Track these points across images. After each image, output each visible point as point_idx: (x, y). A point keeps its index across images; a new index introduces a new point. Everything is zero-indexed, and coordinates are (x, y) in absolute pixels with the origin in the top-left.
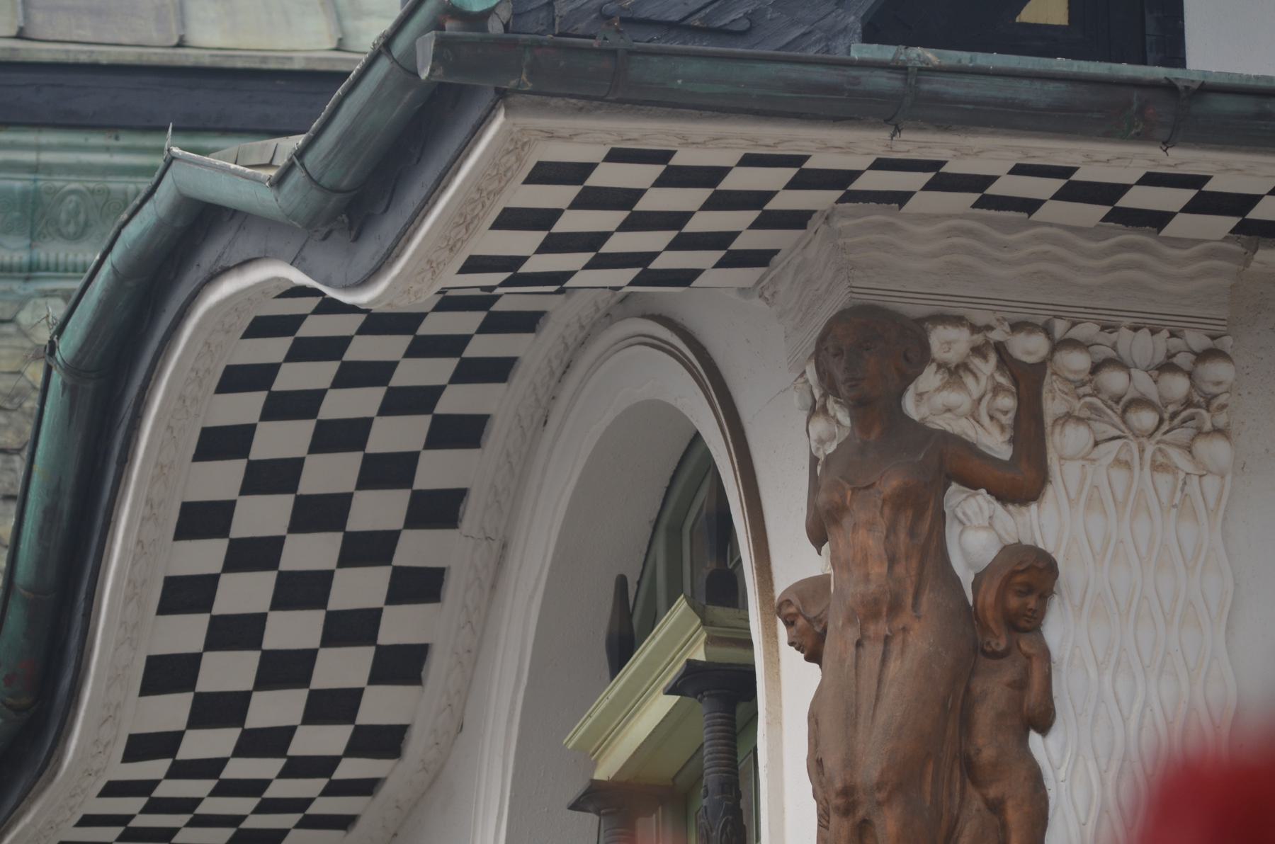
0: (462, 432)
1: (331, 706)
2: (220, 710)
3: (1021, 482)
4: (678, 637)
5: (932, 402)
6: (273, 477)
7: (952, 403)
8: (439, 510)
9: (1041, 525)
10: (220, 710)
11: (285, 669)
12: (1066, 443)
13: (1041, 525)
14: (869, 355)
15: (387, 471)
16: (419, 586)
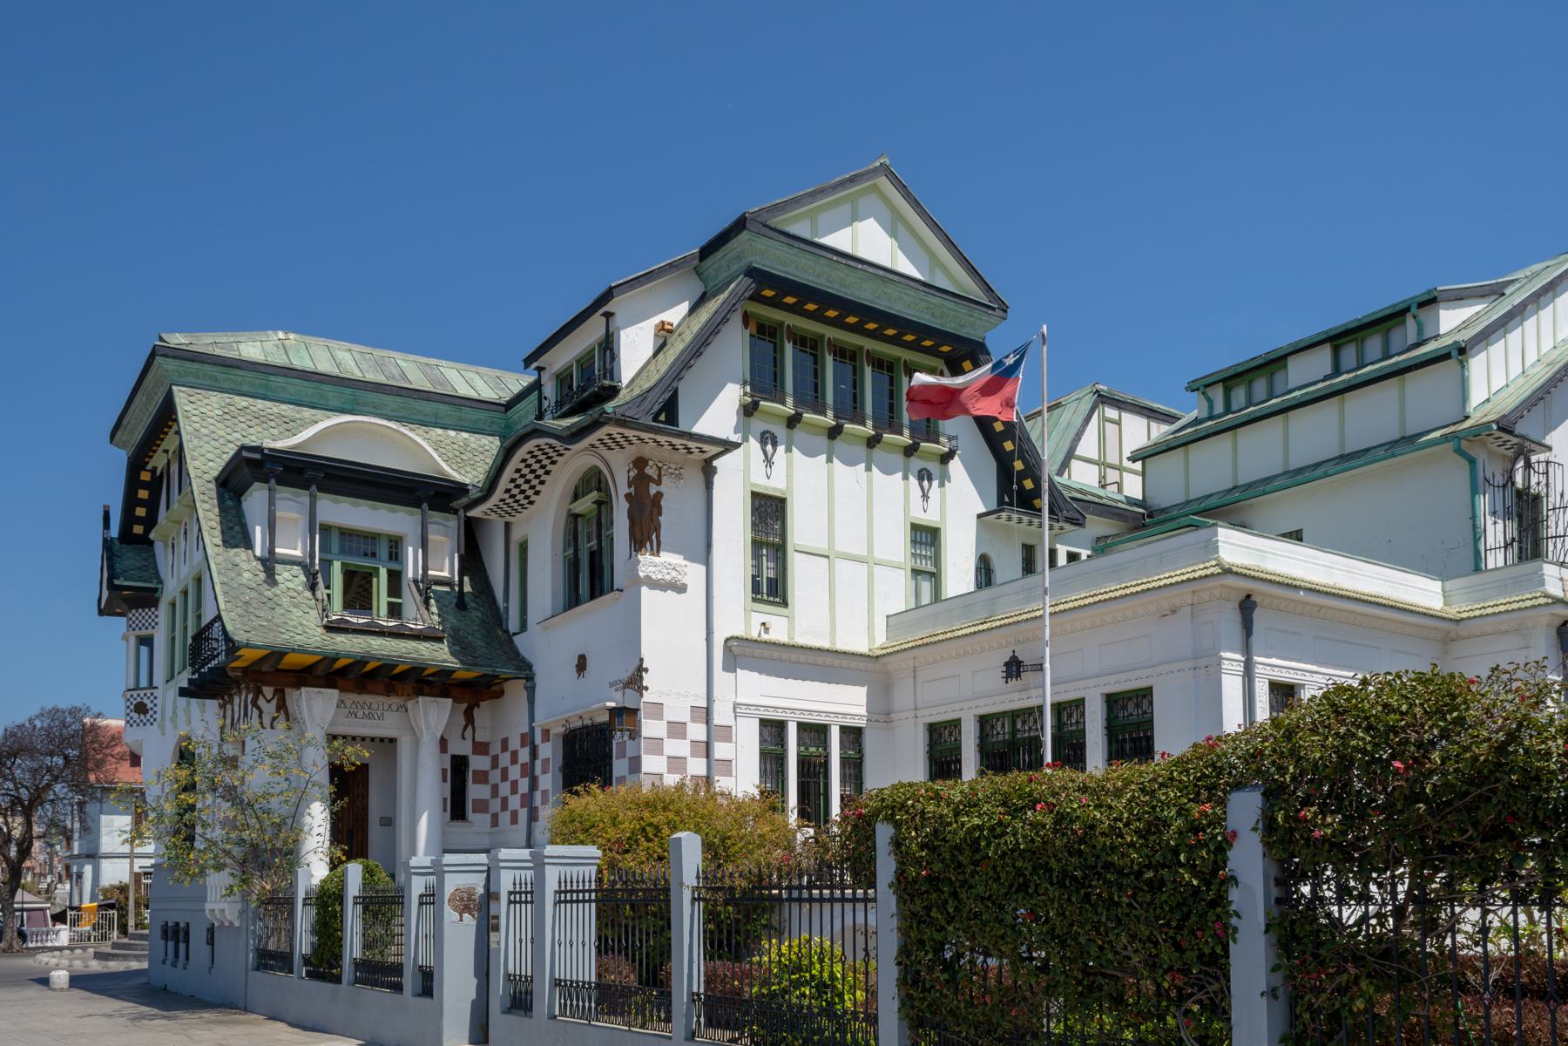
0: (554, 463)
1: (527, 497)
2: (512, 496)
3: (659, 483)
4: (594, 495)
5: (648, 471)
6: (528, 466)
7: (651, 471)
8: (547, 473)
9: (662, 488)
10: (512, 496)
11: (523, 492)
12: (664, 479)
13: (662, 488)
14: (640, 463)
15: (543, 467)
16: (542, 483)
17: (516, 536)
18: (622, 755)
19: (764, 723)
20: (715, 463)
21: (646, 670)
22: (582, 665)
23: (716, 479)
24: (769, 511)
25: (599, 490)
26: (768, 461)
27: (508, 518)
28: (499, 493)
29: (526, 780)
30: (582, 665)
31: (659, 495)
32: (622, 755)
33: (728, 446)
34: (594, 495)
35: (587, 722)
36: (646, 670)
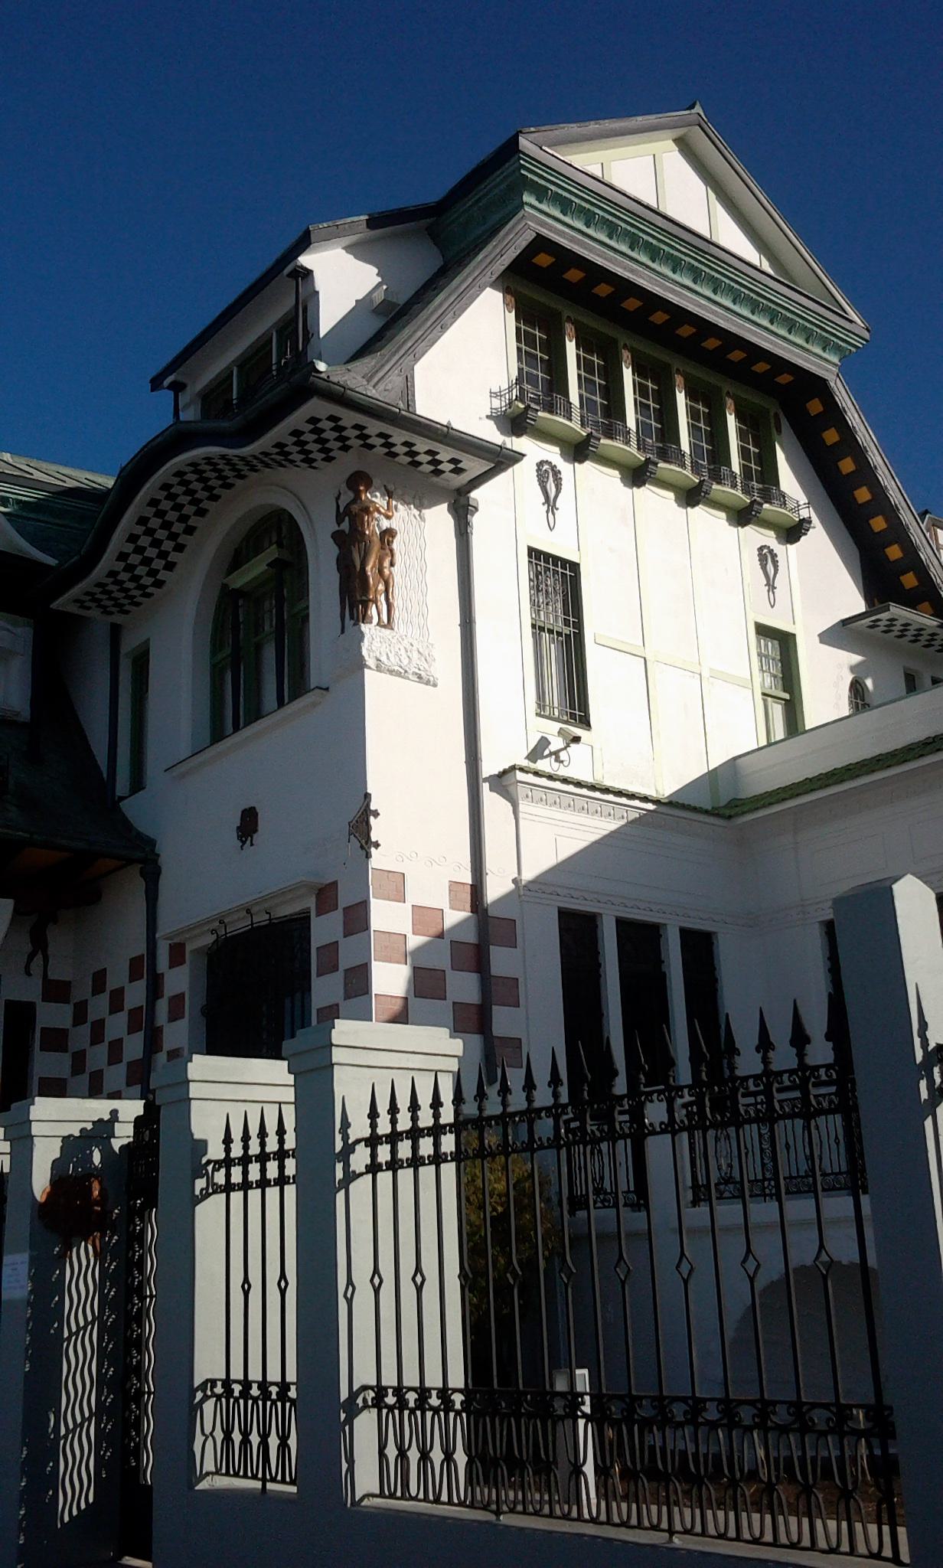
2: (130, 568)
4: (272, 553)
13: (393, 524)
17: (129, 643)
18: (330, 965)
19: (565, 915)
20: (474, 494)
21: (376, 814)
22: (248, 824)
23: (476, 521)
24: (557, 580)
25: (280, 545)
26: (550, 504)
27: (118, 619)
28: (108, 561)
29: (140, 1036)
30: (248, 824)
31: (389, 534)
32: (330, 965)
33: (502, 460)
34: (272, 553)
35: (261, 919)
36: (376, 814)
